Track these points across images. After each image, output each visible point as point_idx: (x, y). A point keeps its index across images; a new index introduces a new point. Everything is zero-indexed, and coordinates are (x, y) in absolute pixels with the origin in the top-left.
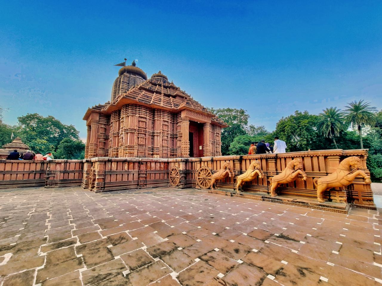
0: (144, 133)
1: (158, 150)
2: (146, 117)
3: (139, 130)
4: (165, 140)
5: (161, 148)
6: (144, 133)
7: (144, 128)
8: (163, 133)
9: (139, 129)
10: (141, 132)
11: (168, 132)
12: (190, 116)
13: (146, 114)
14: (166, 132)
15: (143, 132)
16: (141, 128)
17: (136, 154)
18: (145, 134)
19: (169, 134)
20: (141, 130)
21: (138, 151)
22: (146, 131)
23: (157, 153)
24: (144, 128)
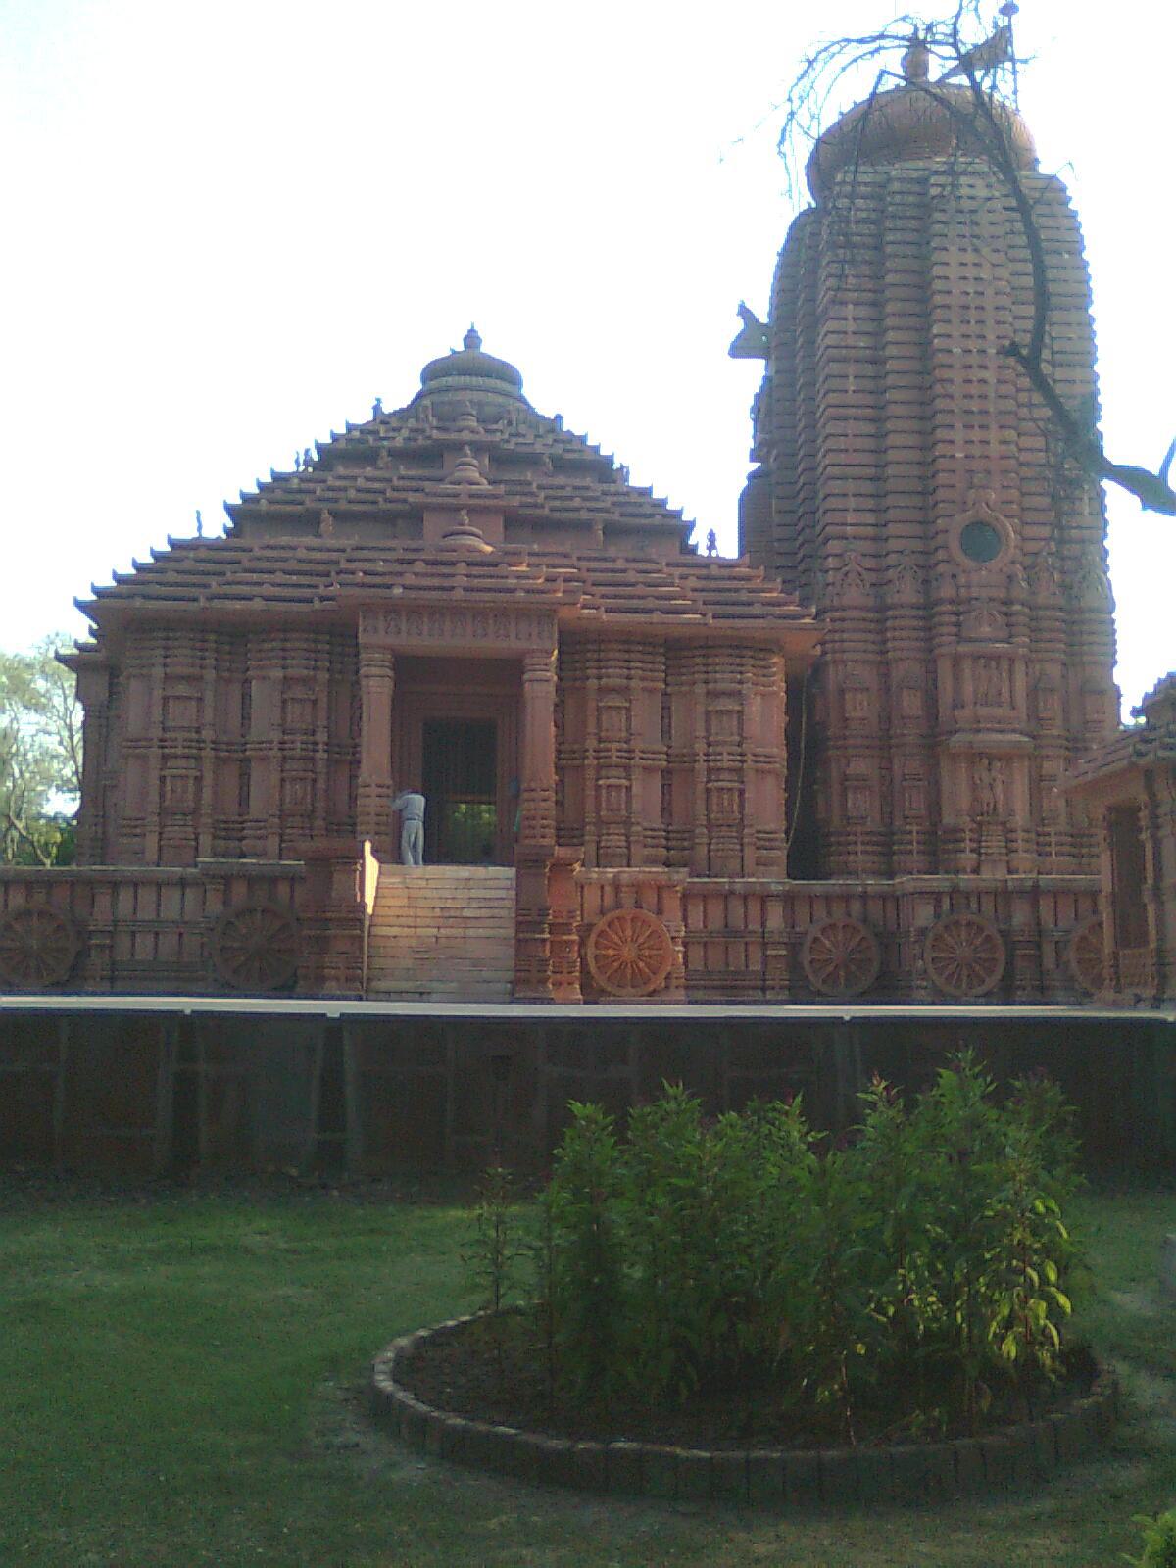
2: (196, 671)
4: (294, 780)
5: (272, 819)
7: (188, 729)
8: (283, 742)
12: (390, 640)
14: (299, 737)
15: (180, 751)
16: (175, 729)
17: (151, 854)
18: (198, 758)
19: (321, 746)
24: (188, 729)
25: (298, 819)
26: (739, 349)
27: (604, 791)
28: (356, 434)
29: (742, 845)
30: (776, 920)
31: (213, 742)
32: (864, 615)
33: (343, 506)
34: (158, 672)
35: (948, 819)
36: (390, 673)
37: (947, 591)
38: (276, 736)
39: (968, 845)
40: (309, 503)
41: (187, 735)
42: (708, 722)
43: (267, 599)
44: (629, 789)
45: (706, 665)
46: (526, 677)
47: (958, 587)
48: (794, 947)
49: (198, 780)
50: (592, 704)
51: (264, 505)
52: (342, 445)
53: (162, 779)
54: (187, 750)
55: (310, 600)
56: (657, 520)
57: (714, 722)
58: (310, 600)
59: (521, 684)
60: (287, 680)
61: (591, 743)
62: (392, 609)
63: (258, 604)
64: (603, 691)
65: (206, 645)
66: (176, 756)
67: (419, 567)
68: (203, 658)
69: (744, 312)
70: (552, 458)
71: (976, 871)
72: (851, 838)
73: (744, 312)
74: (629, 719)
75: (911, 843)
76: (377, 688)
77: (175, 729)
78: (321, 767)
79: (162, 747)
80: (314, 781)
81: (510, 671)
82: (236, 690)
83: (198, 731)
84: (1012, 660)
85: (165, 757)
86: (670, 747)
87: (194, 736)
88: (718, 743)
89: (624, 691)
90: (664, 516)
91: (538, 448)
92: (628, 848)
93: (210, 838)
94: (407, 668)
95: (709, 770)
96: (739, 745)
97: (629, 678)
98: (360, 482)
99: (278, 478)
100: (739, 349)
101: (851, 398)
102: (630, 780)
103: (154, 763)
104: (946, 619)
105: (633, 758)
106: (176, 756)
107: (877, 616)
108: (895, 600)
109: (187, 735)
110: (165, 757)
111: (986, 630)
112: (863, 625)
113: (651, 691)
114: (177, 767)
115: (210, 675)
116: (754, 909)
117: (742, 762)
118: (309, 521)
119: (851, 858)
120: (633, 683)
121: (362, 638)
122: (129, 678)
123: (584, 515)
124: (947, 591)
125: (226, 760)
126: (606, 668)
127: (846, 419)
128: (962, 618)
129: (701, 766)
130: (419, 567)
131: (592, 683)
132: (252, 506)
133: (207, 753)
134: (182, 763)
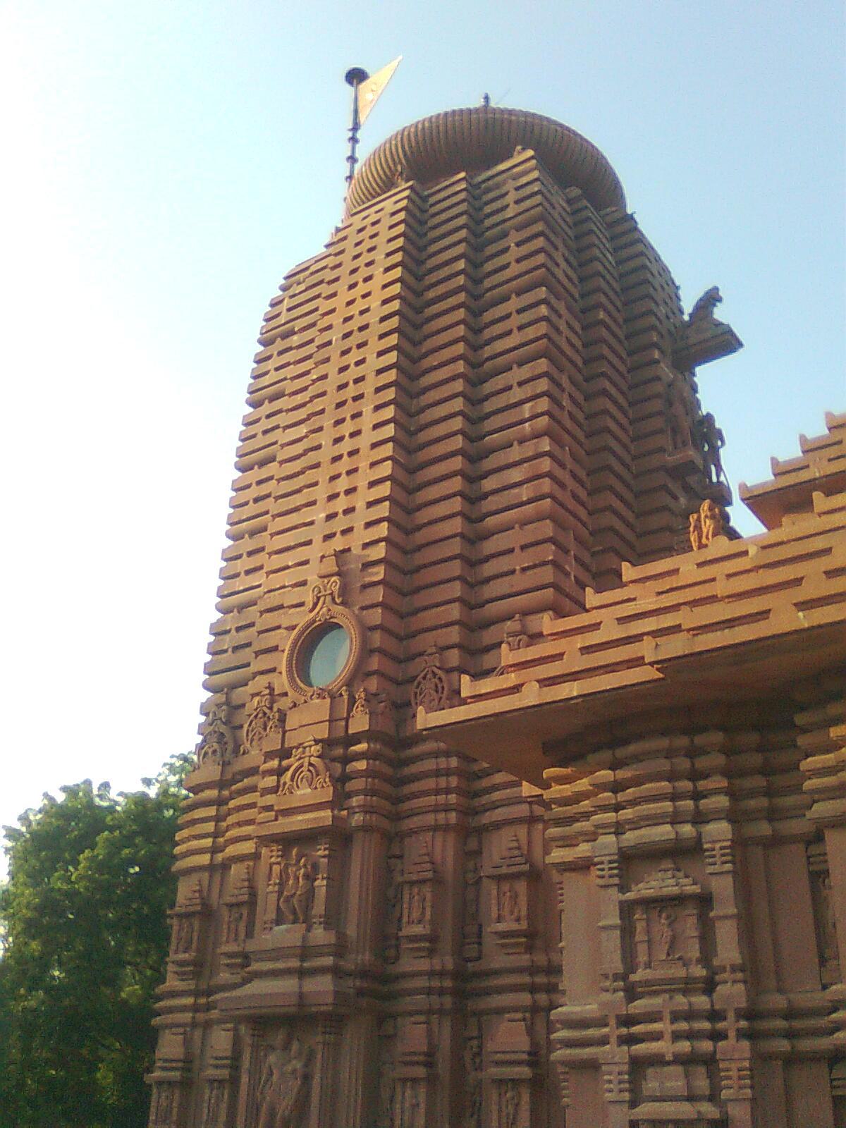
3: (628, 1021)
6: (685, 1046)
7: (688, 986)
9: (640, 1005)
13: (697, 796)
16: (652, 989)
18: (710, 1062)
22: (715, 1015)
24: (688, 986)
31: (740, 1015)
41: (681, 1001)
65: (702, 763)
68: (697, 796)
77: (652, 989)
79: (630, 1040)
82: (793, 864)
83: (709, 986)
87: (701, 1001)
109: (681, 1001)
110: (638, 1066)
133: (735, 1052)
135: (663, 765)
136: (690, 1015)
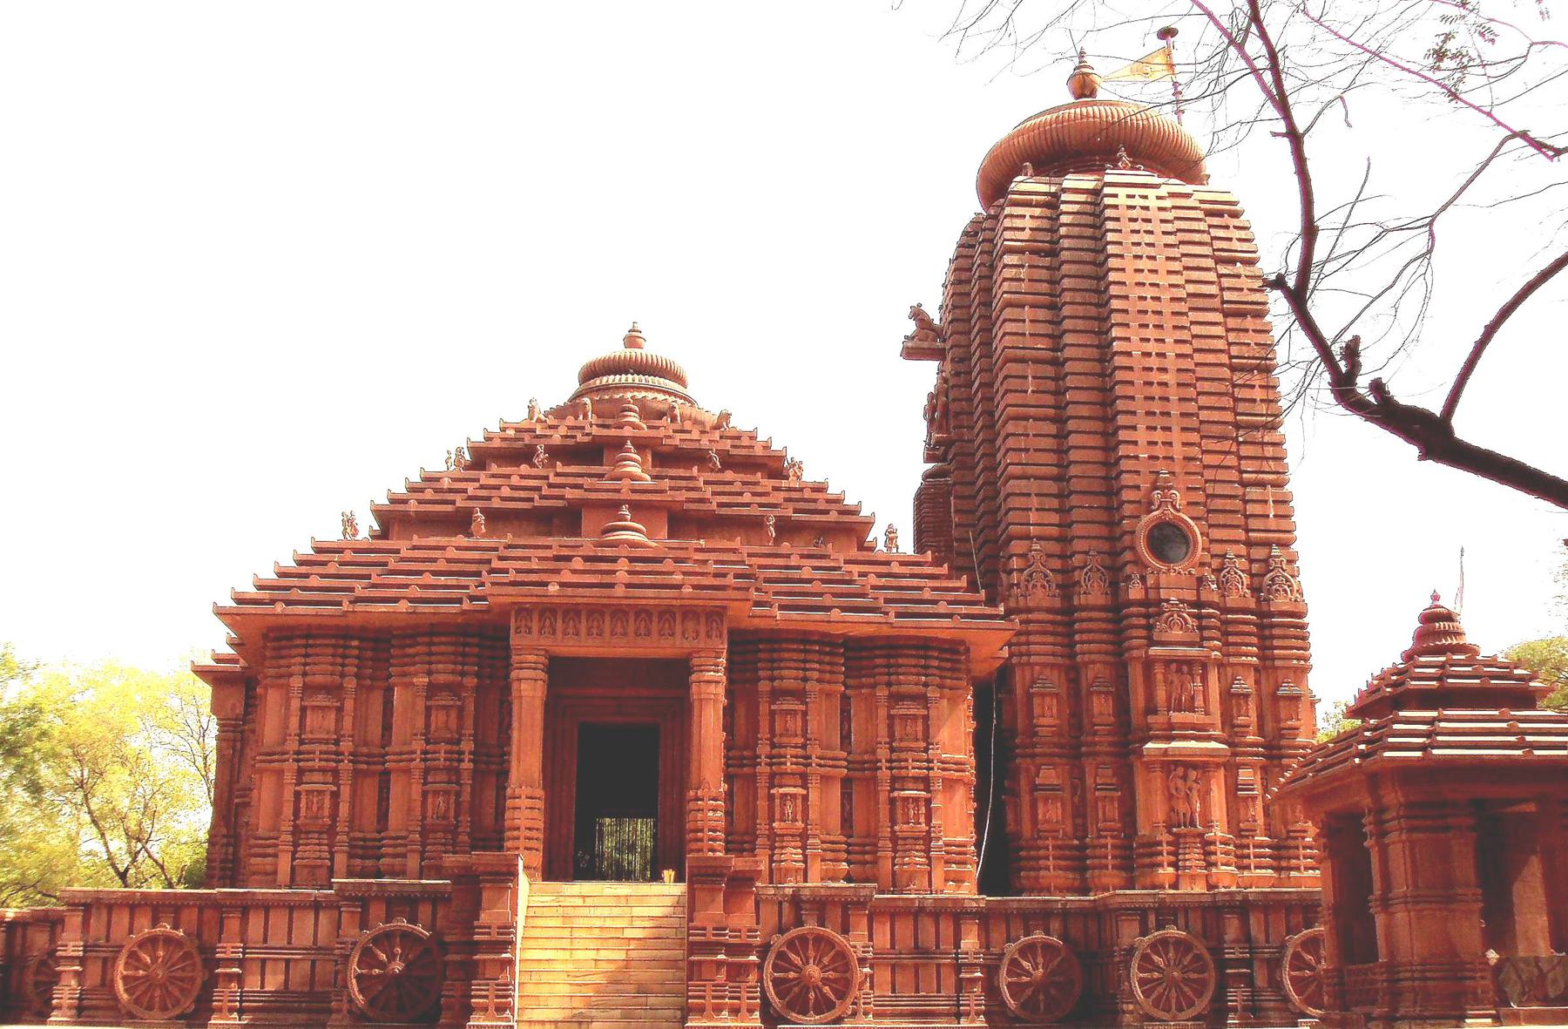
0: (324, 763)
1: (400, 850)
4: (436, 793)
7: (327, 742)
10: (310, 763)
11: (458, 742)
12: (546, 642)
13: (343, 665)
14: (443, 747)
15: (317, 764)
16: (311, 742)
18: (336, 773)
20: (309, 753)
21: (294, 859)
22: (338, 753)
23: (397, 868)
24: (327, 742)
25: (440, 835)
26: (912, 352)
27: (777, 801)
28: (511, 433)
29: (929, 858)
30: (970, 942)
31: (351, 754)
32: (1051, 617)
33: (496, 503)
34: (297, 682)
35: (1143, 830)
36: (542, 675)
37: (1136, 592)
38: (418, 745)
39: (1166, 858)
40: (460, 502)
41: (324, 747)
42: (891, 727)
43: (411, 600)
44: (805, 798)
45: (888, 666)
46: (694, 677)
47: (1146, 590)
48: (991, 970)
49: (335, 796)
50: (764, 708)
51: (413, 506)
52: (497, 443)
53: (297, 795)
54: (324, 763)
55: (459, 601)
56: (833, 516)
57: (897, 728)
58: (459, 601)
59: (688, 687)
60: (432, 690)
61: (763, 749)
62: (548, 611)
63: (403, 606)
64: (776, 695)
66: (312, 770)
67: (578, 564)
69: (918, 314)
70: (718, 452)
71: (1175, 886)
72: (1042, 852)
73: (918, 314)
74: (805, 722)
75: (1106, 857)
76: (529, 691)
77: (311, 742)
78: (467, 780)
80: (458, 794)
81: (679, 671)
82: (377, 700)
83: (337, 742)
84: (1204, 666)
85: (301, 772)
86: (849, 753)
87: (333, 747)
88: (902, 750)
89: (800, 695)
90: (841, 513)
91: (705, 443)
92: (805, 861)
93: (345, 856)
94: (559, 670)
95: (894, 779)
96: (926, 750)
97: (805, 679)
98: (515, 480)
99: (430, 479)
100: (912, 352)
101: (1030, 398)
102: (807, 789)
103: (289, 778)
104: (1135, 621)
105: (810, 765)
106: (312, 770)
107: (1066, 619)
108: (1083, 601)
109: (324, 747)
111: (1177, 634)
112: (1050, 628)
113: (829, 695)
114: (315, 782)
115: (350, 684)
116: (947, 928)
117: (929, 769)
118: (459, 522)
119: (1042, 873)
120: (809, 686)
121: (514, 640)
122: (266, 688)
123: (755, 511)
124: (1136, 592)
125: (365, 774)
126: (780, 668)
127: (1026, 418)
128: (1151, 621)
129: (884, 774)
130: (578, 564)
131: (764, 686)
132: (401, 507)
133: (346, 765)
134: (317, 777)
135: (330, 650)
136: (326, 753)
